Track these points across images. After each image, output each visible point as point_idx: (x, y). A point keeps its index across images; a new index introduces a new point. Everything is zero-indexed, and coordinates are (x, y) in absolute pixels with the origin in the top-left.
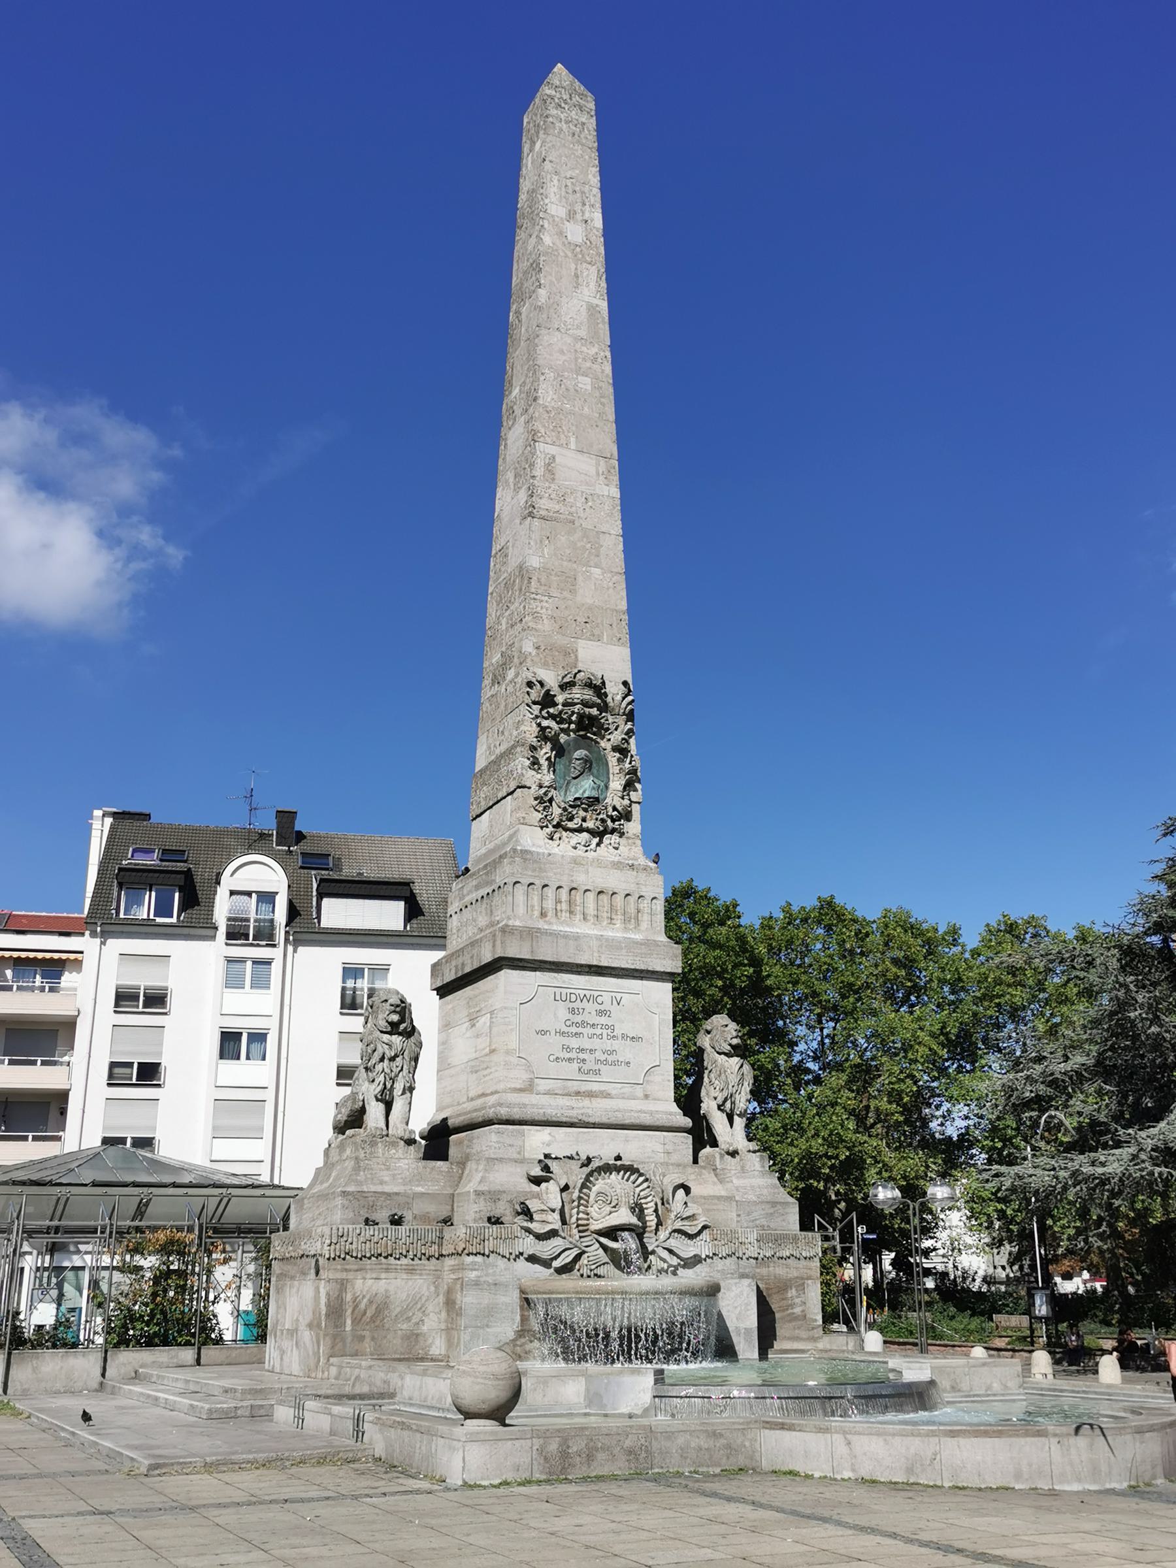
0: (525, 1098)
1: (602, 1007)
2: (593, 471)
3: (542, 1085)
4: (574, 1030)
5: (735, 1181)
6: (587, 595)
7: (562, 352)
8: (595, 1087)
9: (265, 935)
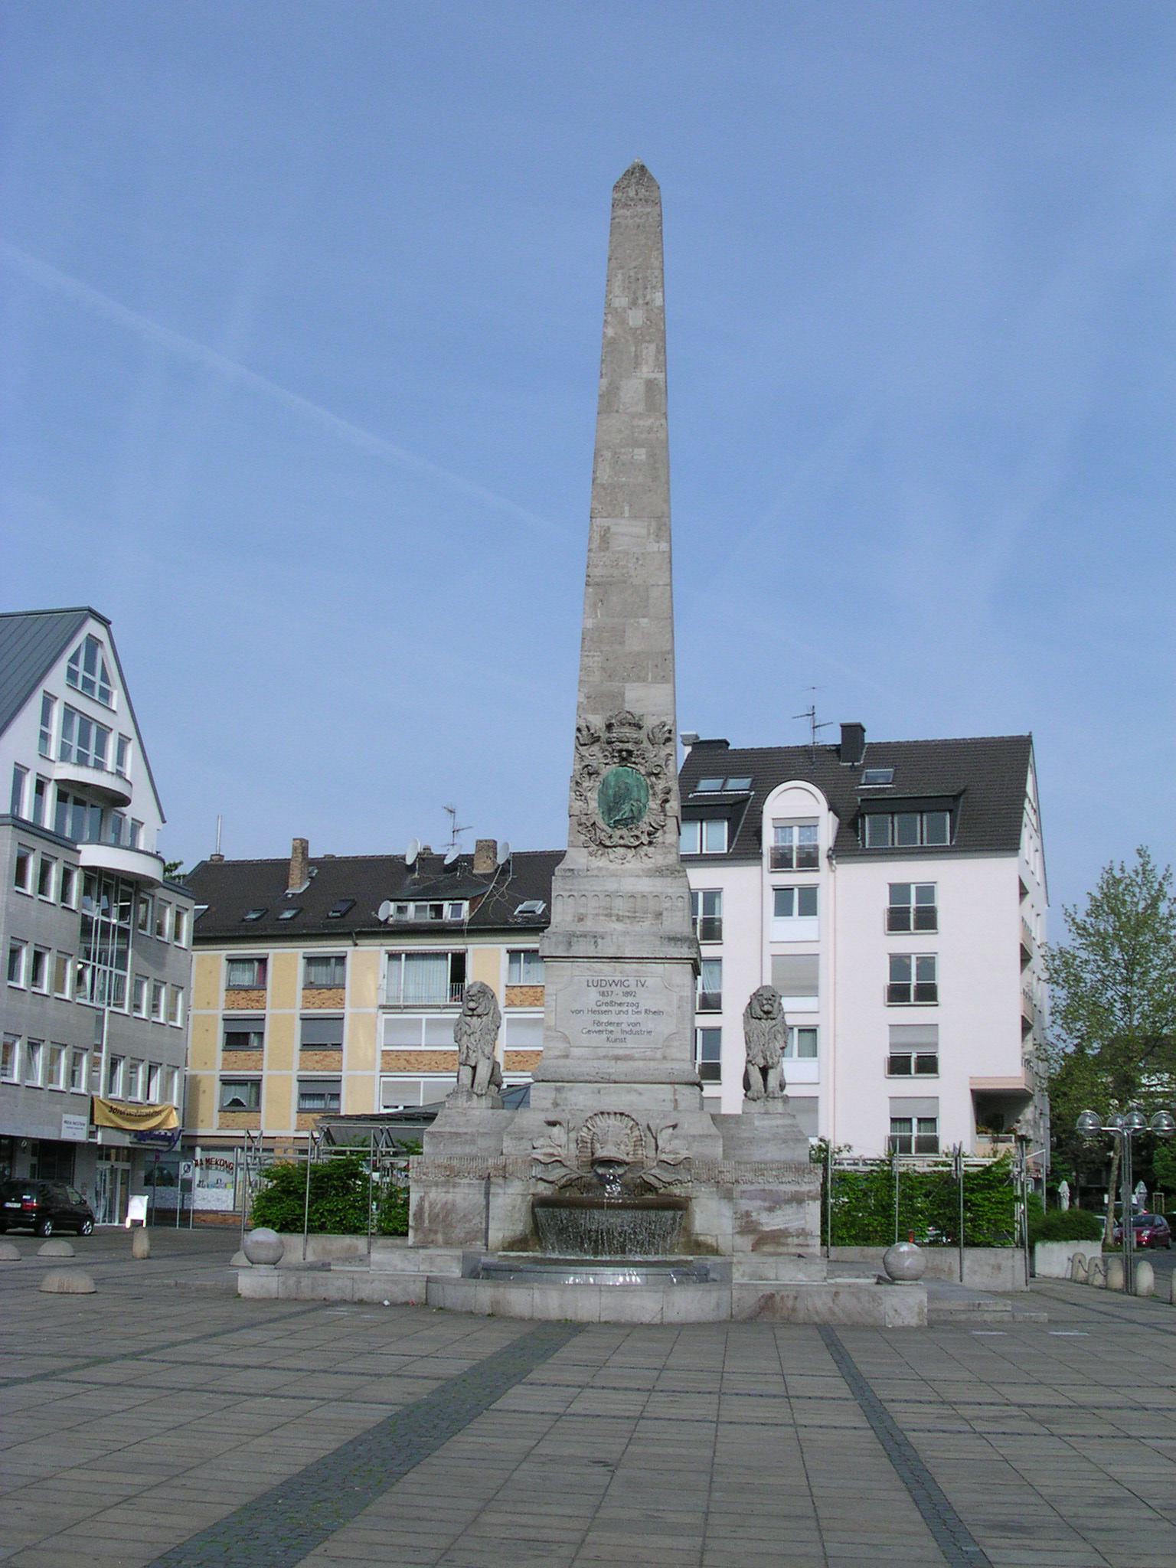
0: (562, 1062)
2: (644, 532)
3: (576, 1052)
4: (604, 1008)
5: (757, 1123)
6: (634, 644)
7: (620, 431)
8: (621, 1052)
9: (809, 861)
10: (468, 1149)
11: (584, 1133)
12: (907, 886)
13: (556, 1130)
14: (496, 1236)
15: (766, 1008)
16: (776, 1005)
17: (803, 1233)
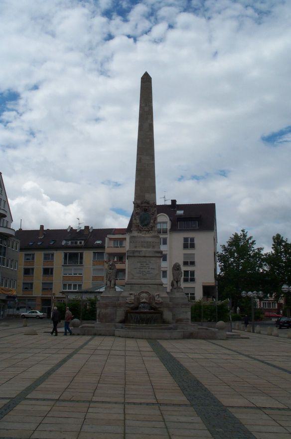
12: (188, 238)
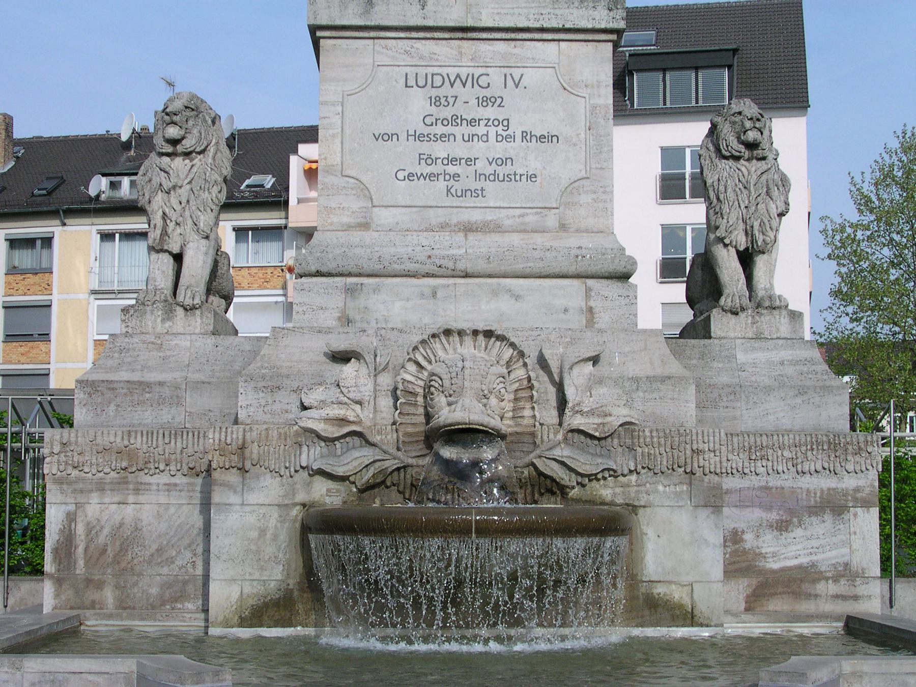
0: (357, 236)
1: (488, 93)
3: (384, 217)
4: (439, 129)
5: (741, 357)
8: (476, 216)
10: (167, 415)
11: (410, 374)
12: (682, 149)
13: (349, 370)
14: (225, 594)
15: (752, 136)
16: (766, 132)
17: (847, 572)
